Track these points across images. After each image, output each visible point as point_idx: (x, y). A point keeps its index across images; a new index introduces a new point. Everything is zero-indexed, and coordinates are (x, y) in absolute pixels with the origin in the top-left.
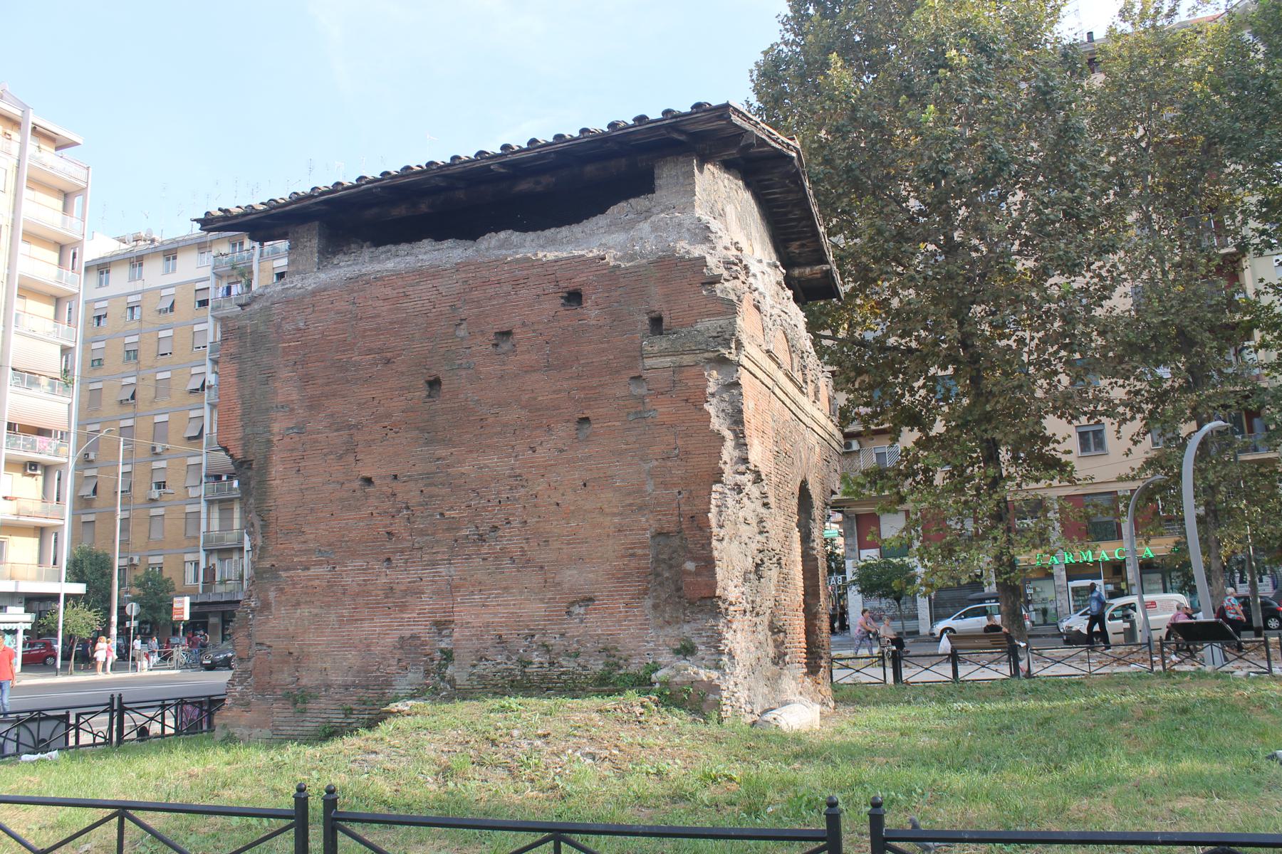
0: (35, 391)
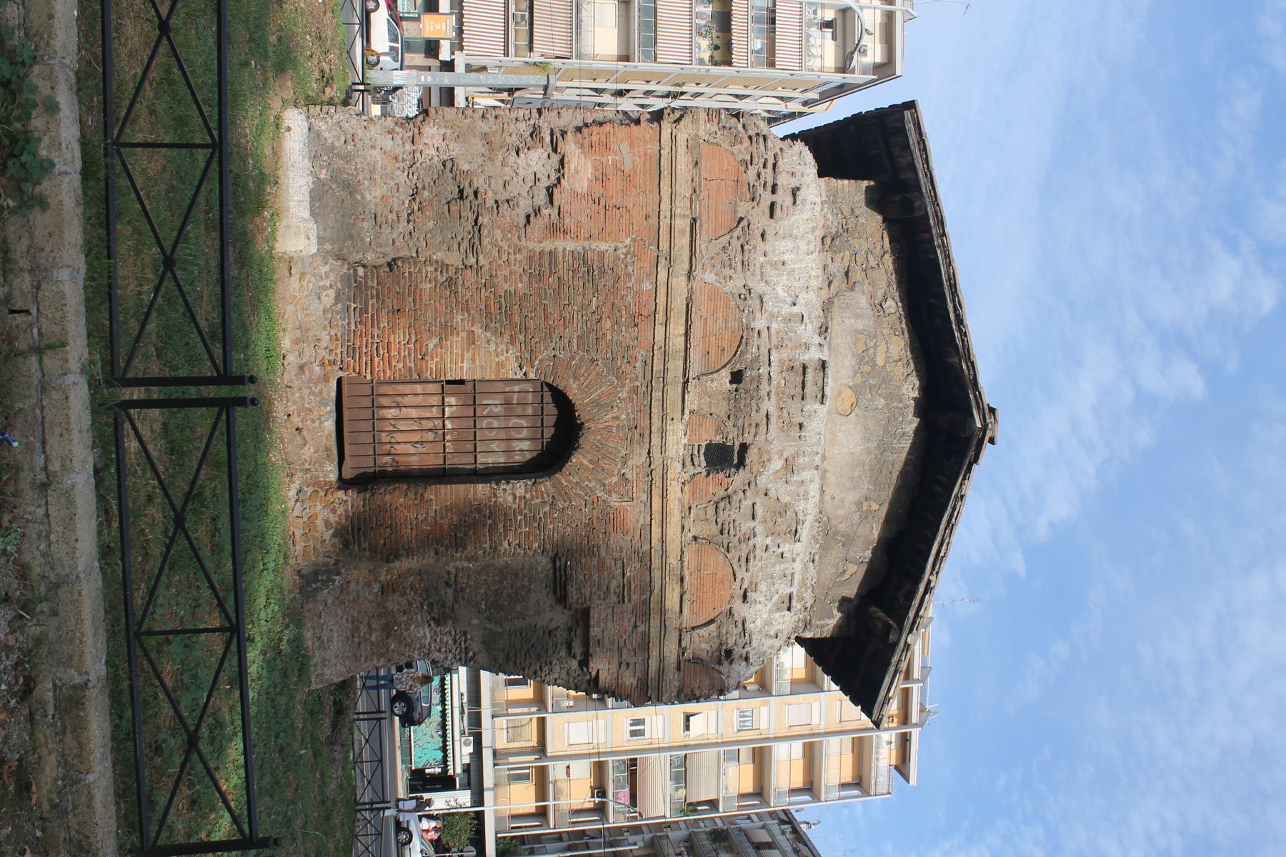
0: (670, 786)
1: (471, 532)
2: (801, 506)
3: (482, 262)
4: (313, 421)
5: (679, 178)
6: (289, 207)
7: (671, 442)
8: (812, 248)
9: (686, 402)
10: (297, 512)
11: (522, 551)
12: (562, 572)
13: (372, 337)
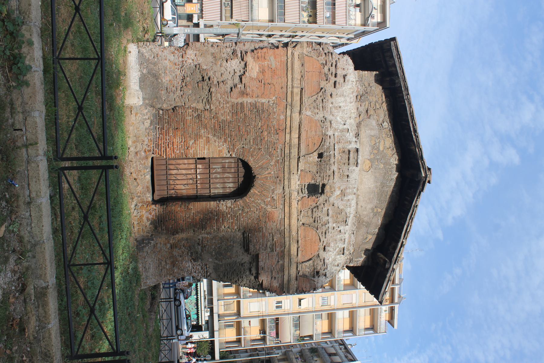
0: (293, 329)
1: (208, 222)
2: (348, 210)
3: (212, 107)
4: (141, 176)
5: (295, 71)
6: (130, 85)
7: (293, 183)
8: (352, 100)
9: (299, 166)
10: (135, 214)
11: (230, 230)
12: (247, 239)
13: (166, 140)
